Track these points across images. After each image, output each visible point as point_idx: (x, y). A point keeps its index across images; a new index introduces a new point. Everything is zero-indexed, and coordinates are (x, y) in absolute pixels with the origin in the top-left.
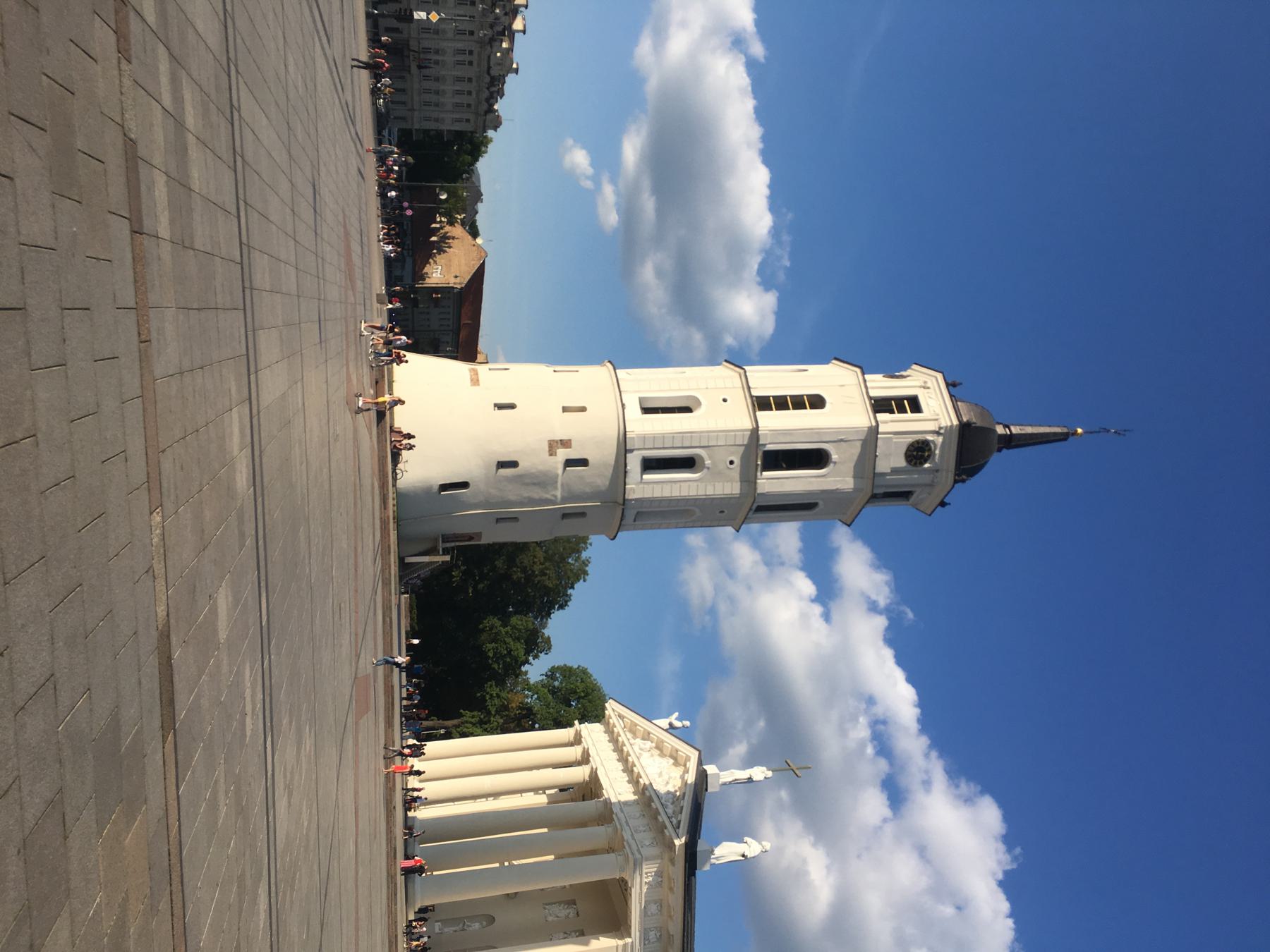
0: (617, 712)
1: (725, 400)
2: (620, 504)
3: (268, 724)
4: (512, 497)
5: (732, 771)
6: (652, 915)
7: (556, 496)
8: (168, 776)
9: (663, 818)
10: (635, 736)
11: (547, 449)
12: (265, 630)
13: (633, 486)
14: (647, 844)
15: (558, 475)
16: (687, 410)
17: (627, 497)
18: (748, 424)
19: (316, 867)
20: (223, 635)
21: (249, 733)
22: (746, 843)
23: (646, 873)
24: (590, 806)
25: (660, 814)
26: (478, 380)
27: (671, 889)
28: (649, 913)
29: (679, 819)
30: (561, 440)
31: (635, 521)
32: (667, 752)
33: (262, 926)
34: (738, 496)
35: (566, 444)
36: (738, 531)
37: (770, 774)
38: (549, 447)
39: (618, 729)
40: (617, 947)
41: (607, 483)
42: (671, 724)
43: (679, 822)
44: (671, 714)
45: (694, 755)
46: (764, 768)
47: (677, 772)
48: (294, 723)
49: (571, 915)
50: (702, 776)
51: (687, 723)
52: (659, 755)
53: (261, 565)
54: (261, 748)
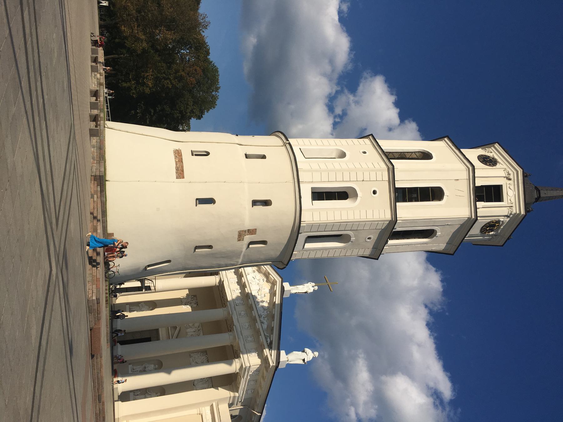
1: (375, 192)
4: (204, 265)
5: (298, 286)
7: (238, 262)
9: (262, 339)
11: (237, 237)
13: (296, 253)
15: (242, 252)
18: (388, 216)
22: (306, 353)
27: (263, 377)
28: (250, 384)
35: (252, 232)
40: (230, 397)
41: (278, 253)
43: (271, 343)
46: (314, 284)
47: (267, 287)
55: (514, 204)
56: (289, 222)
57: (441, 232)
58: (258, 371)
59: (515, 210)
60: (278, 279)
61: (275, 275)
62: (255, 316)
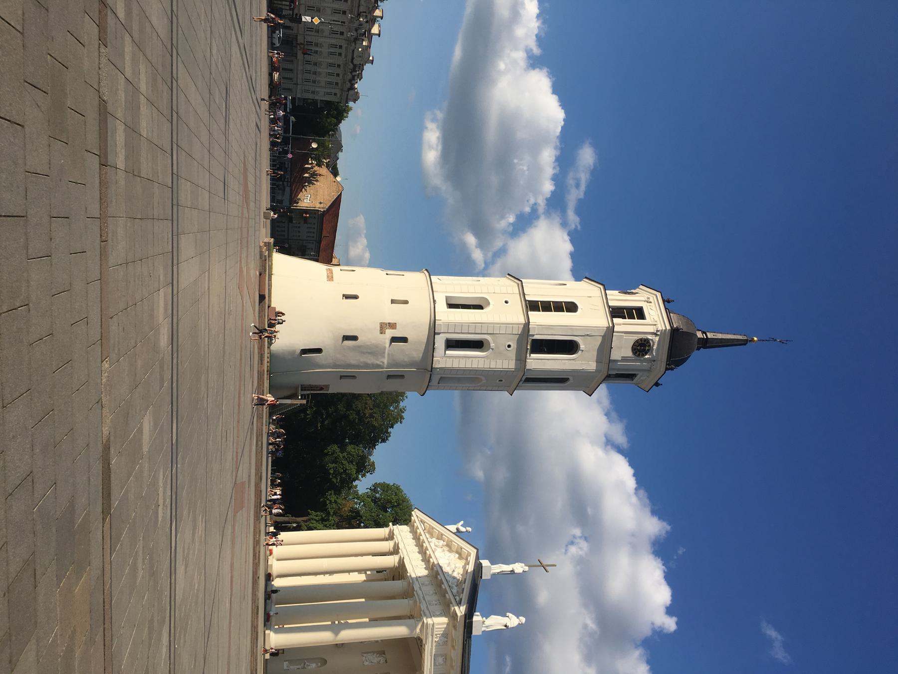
0: (420, 518)
1: (506, 302)
2: (429, 371)
3: (174, 514)
4: (353, 362)
5: (500, 565)
6: (440, 665)
7: (383, 363)
8: (105, 547)
9: (449, 596)
10: (432, 536)
12: (174, 447)
14: (438, 614)
15: (385, 348)
16: (480, 307)
17: (434, 367)
18: (522, 320)
19: (202, 616)
20: (145, 449)
21: (160, 519)
22: (508, 617)
23: (436, 635)
24: (398, 585)
25: (447, 593)
26: (332, 277)
27: (453, 647)
29: (461, 597)
30: (389, 323)
31: (439, 383)
32: (454, 549)
33: (163, 657)
34: (514, 370)
35: (392, 326)
36: (511, 395)
37: (527, 569)
38: (380, 328)
39: (420, 530)
41: (421, 355)
42: (457, 529)
44: (459, 522)
45: (473, 552)
46: (523, 565)
47: (461, 564)
48: (191, 513)
49: (382, 662)
50: (479, 567)
51: (469, 529)
52: (448, 551)
53: (174, 401)
54: (168, 530)
55: (658, 321)
56: (426, 320)
57: (584, 345)
58: (445, 635)
59: (661, 327)
60: (472, 551)
61: (467, 547)
62: (446, 589)
